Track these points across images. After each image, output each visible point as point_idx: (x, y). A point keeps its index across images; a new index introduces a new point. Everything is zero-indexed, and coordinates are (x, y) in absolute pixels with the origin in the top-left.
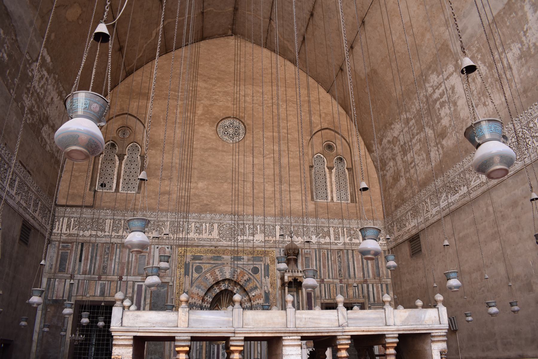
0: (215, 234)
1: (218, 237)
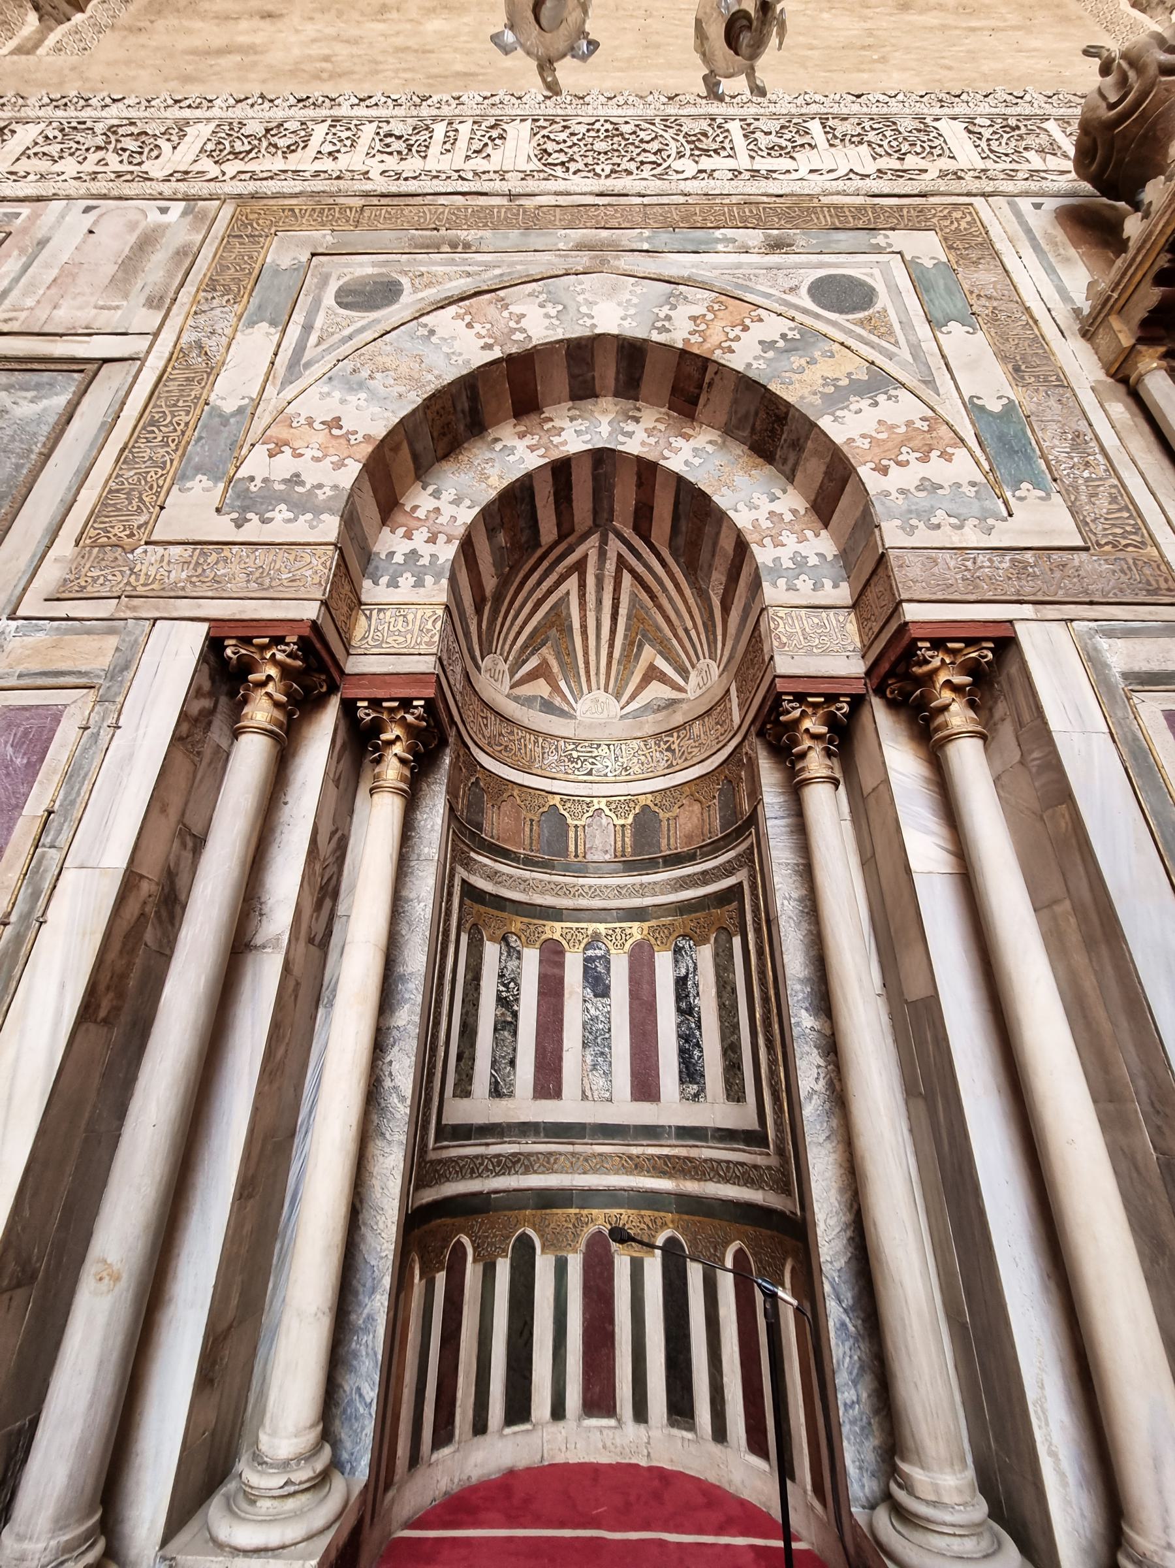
0: (517, 149)
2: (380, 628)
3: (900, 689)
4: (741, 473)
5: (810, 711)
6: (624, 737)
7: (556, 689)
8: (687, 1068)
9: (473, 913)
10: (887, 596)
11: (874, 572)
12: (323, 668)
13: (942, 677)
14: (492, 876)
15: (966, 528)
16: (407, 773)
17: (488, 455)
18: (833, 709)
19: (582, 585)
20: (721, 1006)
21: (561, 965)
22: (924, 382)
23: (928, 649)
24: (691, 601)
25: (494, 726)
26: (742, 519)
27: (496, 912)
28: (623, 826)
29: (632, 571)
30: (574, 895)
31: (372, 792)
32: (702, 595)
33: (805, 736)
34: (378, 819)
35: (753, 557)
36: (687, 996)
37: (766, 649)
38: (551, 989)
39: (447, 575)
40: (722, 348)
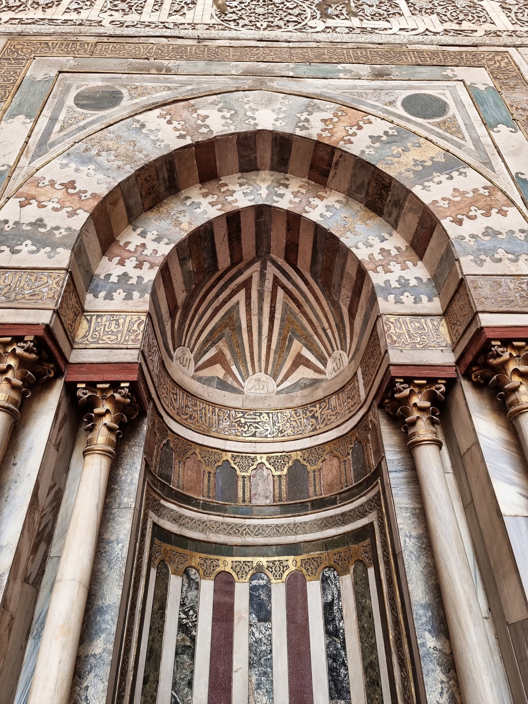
1: (216, 20)
2: (98, 329)
3: (481, 375)
4: (360, 222)
5: (416, 390)
6: (279, 407)
7: (229, 371)
8: (335, 685)
9: (163, 550)
10: (467, 308)
11: (457, 291)
12: (52, 359)
13: (512, 366)
14: (177, 519)
15: (520, 261)
16: (113, 438)
17: (181, 208)
18: (433, 388)
19: (248, 298)
20: (361, 629)
21: (231, 594)
22: (484, 163)
23: (499, 346)
24: (327, 309)
25: (182, 400)
26: (362, 253)
27: (180, 550)
28: (280, 476)
29: (284, 288)
30: (242, 534)
31: (85, 453)
32: (335, 305)
33: (414, 409)
34: (89, 475)
35: (370, 279)
36: (334, 619)
37: (382, 345)
38: (223, 615)
39: (150, 291)
40: (344, 140)
